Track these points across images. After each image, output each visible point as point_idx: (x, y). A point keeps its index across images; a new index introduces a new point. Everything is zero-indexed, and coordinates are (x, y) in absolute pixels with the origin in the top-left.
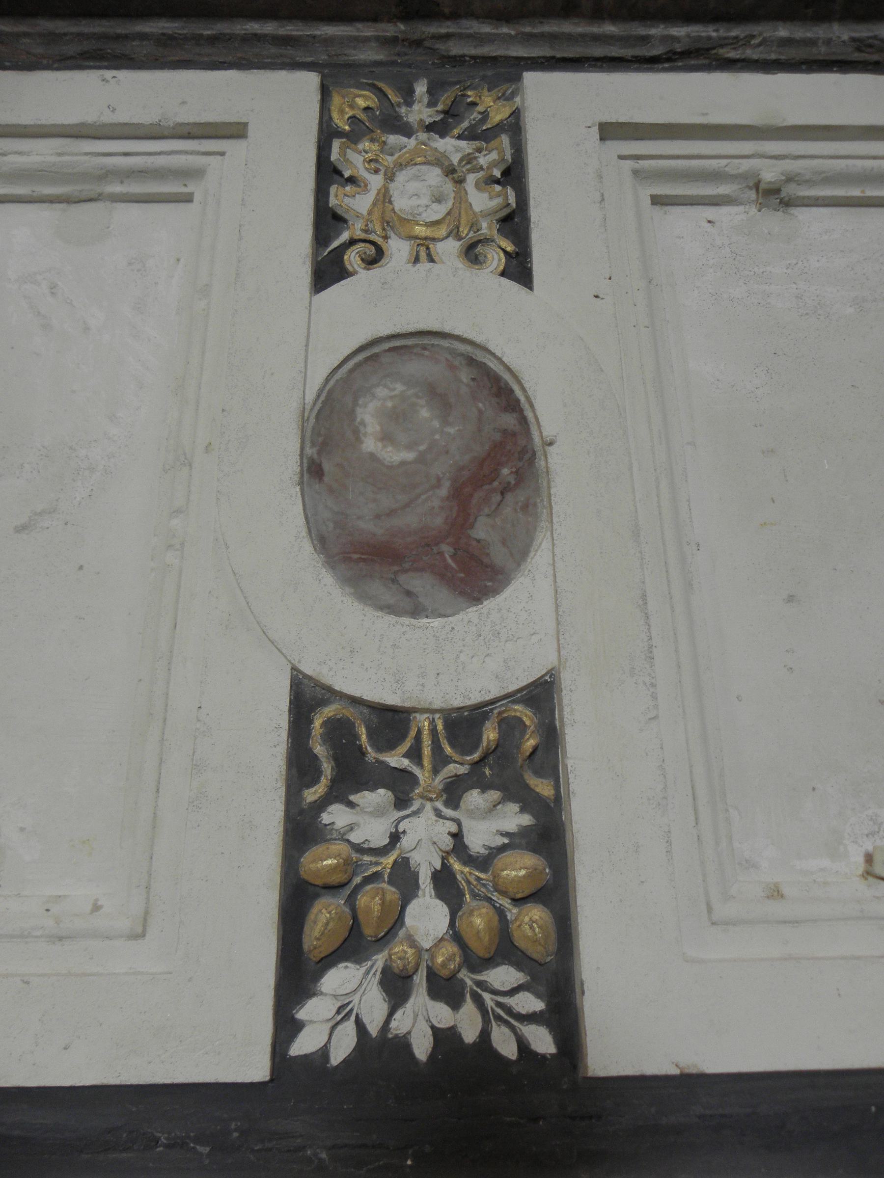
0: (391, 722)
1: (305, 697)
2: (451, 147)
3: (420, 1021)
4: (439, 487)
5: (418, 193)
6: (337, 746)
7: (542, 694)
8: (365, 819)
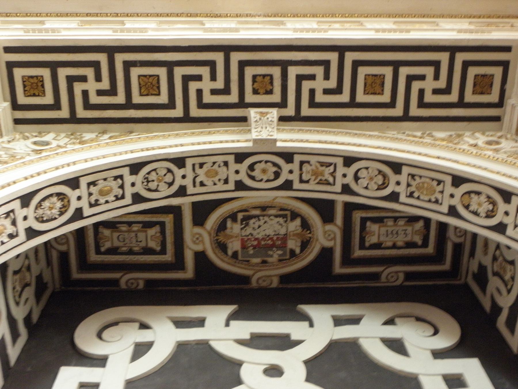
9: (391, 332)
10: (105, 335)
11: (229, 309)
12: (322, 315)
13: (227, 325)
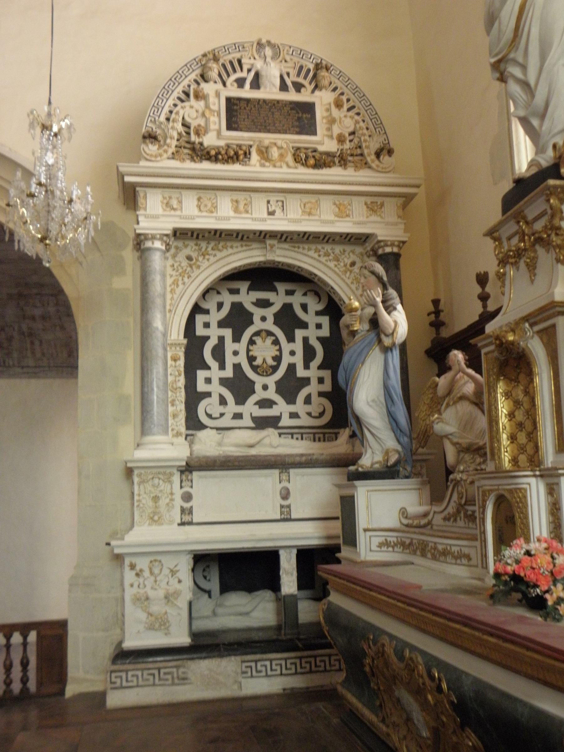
4: (286, 494)
5: (284, 478)
6: (282, 507)
8: (283, 509)
9: (304, 300)
10: (206, 297)
12: (281, 287)
13: (248, 293)
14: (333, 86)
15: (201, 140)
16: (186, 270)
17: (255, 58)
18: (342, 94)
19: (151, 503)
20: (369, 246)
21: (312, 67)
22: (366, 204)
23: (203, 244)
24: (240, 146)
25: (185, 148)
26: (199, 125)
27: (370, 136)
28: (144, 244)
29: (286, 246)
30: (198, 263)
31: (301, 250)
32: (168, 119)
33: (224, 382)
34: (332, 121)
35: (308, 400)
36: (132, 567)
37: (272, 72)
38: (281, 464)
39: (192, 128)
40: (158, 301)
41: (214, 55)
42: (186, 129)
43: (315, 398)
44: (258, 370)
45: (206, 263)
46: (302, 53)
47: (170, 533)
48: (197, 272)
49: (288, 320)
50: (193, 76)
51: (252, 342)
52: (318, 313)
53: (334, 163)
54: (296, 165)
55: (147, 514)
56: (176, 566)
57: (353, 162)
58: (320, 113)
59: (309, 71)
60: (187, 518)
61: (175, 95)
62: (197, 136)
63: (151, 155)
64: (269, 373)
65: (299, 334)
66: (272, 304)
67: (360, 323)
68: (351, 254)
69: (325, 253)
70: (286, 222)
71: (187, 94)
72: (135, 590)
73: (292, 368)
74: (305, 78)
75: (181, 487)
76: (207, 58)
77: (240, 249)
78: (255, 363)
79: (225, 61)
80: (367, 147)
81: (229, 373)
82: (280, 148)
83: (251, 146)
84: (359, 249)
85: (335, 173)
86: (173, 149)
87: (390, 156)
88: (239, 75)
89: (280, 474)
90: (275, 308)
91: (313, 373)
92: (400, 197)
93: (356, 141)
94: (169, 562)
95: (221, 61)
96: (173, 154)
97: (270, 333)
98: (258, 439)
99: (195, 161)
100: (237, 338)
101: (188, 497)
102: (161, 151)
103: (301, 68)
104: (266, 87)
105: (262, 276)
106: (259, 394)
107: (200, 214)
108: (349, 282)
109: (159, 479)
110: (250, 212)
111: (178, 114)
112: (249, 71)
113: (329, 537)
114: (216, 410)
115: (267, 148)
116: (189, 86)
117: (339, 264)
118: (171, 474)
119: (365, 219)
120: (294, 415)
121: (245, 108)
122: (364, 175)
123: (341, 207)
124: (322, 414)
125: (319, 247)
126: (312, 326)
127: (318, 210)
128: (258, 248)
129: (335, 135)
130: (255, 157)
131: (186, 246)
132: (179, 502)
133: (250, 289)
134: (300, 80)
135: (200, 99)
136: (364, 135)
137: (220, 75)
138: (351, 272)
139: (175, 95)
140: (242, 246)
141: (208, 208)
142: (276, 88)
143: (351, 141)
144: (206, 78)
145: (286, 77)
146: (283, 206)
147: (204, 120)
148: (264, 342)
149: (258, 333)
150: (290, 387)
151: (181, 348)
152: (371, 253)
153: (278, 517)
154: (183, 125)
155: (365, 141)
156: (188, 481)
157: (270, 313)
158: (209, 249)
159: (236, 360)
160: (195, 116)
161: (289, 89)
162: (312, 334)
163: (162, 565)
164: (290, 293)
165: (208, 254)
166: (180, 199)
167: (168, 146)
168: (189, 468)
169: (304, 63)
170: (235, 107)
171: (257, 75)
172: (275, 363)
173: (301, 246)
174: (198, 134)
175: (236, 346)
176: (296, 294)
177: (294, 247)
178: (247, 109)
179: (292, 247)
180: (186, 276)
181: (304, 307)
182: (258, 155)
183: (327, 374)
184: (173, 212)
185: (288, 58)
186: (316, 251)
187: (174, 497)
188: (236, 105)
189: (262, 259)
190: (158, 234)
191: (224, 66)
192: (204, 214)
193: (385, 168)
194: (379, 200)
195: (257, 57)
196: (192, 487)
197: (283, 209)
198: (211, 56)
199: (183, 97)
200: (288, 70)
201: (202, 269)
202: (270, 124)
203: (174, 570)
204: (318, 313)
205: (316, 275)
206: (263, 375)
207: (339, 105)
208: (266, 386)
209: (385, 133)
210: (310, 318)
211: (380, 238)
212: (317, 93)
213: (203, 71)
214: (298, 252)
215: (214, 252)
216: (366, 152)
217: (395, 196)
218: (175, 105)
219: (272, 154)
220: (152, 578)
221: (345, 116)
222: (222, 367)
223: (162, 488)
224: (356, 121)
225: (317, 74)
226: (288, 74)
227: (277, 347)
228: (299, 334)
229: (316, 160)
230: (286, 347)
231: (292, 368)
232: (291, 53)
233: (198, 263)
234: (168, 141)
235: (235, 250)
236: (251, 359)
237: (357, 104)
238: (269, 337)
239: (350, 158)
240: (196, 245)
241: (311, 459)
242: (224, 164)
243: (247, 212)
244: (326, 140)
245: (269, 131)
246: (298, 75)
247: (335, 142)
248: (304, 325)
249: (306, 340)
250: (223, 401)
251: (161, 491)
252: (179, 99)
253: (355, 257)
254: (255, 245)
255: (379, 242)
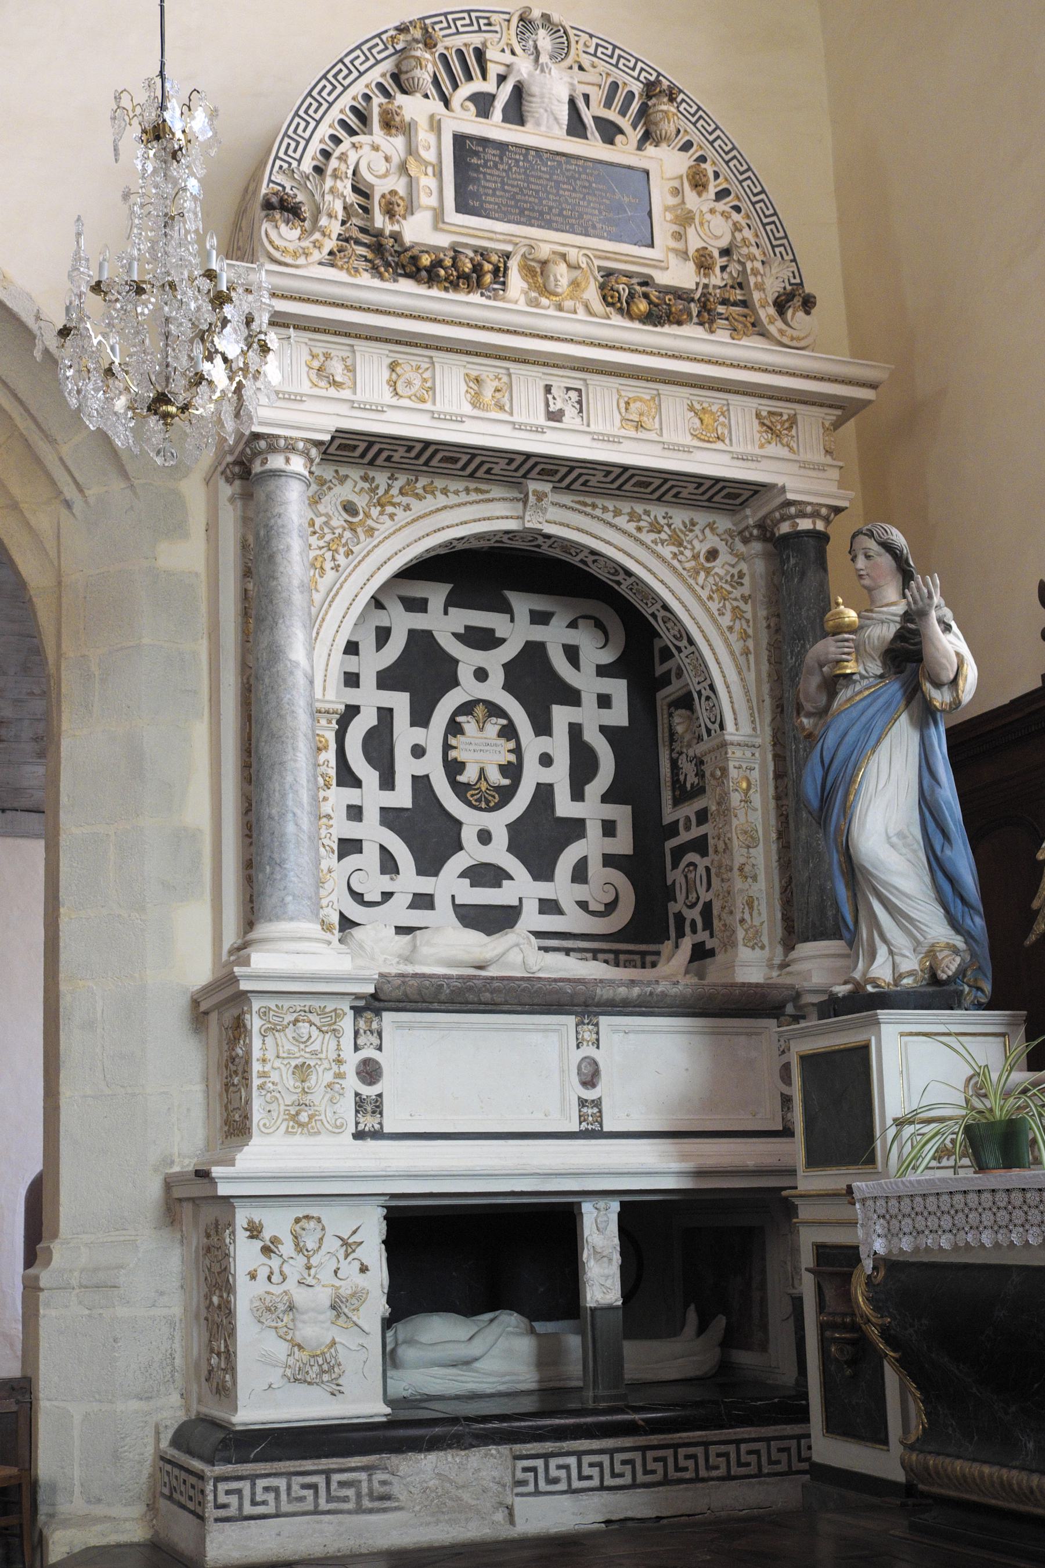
0: (586, 1101)
1: (579, 1098)
2: (590, 1027)
3: (590, 1127)
4: (590, 1077)
5: (587, 1035)
6: (583, 1103)
7: (600, 1098)
8: (585, 1110)
9: (573, 637)
11: (448, 587)
12: (522, 603)
13: (446, 613)
14: (683, 139)
15: (396, 228)
16: (341, 536)
17: (513, 53)
18: (702, 159)
19: (291, 1082)
20: (751, 516)
21: (637, 88)
22: (758, 416)
23: (381, 478)
24: (483, 253)
25: (357, 242)
26: (393, 193)
27: (763, 263)
28: (264, 462)
29: (567, 499)
30: (370, 522)
31: (598, 512)
32: (319, 170)
33: (390, 817)
34: (685, 219)
35: (580, 874)
36: (254, 1231)
37: (554, 88)
38: (580, 1004)
39: (377, 198)
40: (298, 599)
41: (425, 29)
42: (362, 201)
43: (595, 867)
44: (468, 795)
45: (386, 526)
46: (614, 54)
47: (332, 1153)
48: (366, 543)
49: (537, 683)
50: (375, 75)
51: (454, 728)
52: (602, 671)
53: (690, 314)
54: (608, 309)
55: (282, 1108)
56: (354, 1232)
57: (727, 319)
58: (660, 198)
59: (631, 95)
60: (369, 1122)
61: (334, 114)
62: (387, 218)
63: (285, 251)
64: (492, 804)
65: (561, 716)
66: (503, 641)
67: (857, 661)
68: (707, 531)
69: (651, 524)
70: (586, 440)
71: (363, 117)
72: (260, 1286)
73: (544, 793)
74: (623, 113)
75: (357, 1048)
76: (409, 38)
77: (463, 497)
78: (461, 778)
79: (447, 48)
80: (760, 287)
81: (402, 797)
82: (573, 267)
83: (507, 256)
84: (724, 523)
85: (689, 336)
86: (330, 244)
87: (808, 313)
88: (478, 85)
89: (577, 1025)
90: (508, 652)
91: (591, 809)
92: (831, 406)
93: (734, 268)
94: (338, 1221)
95: (440, 49)
96: (331, 253)
97: (495, 710)
98: (499, 950)
99: (381, 277)
100: (421, 717)
101: (370, 1072)
102: (306, 244)
103: (615, 86)
104: (538, 124)
105: (472, 572)
106: (472, 853)
107: (394, 401)
108: (704, 594)
109: (311, 1024)
110: (507, 408)
111: (346, 161)
112: (502, 79)
113: (700, 1173)
114: (373, 885)
115: (544, 263)
116: (367, 98)
117: (682, 553)
118: (338, 1014)
119: (758, 451)
120: (549, 907)
121: (496, 166)
122: (752, 349)
123: (706, 418)
124: (611, 907)
125: (639, 508)
126: (589, 700)
127: (657, 419)
128: (504, 499)
129: (691, 252)
130: (516, 280)
131: (343, 479)
132: (353, 1083)
133: (451, 602)
134: (612, 115)
135: (394, 131)
136: (753, 259)
137: (436, 82)
138: (708, 571)
139: (334, 114)
140: (467, 490)
141: (414, 390)
142: (561, 128)
143: (723, 269)
144: (406, 85)
145: (581, 104)
146: (580, 402)
147: (404, 180)
148: (481, 729)
149: (466, 708)
150: (541, 839)
151: (329, 722)
152: (755, 532)
153: (574, 1127)
154: (356, 189)
155: (755, 272)
156: (372, 1032)
157: (495, 660)
158: (395, 491)
159: (420, 768)
160: (383, 171)
161: (589, 135)
162: (590, 718)
163: (323, 1229)
164: (540, 618)
165: (394, 505)
166: (349, 362)
167: (324, 234)
168: (374, 1004)
169: (620, 77)
170: (474, 160)
171: (519, 91)
172: (506, 782)
173: (599, 502)
174: (390, 212)
175: (418, 735)
176: (554, 621)
177: (585, 504)
178: (501, 167)
179: (579, 502)
180: (342, 550)
181: (572, 654)
182: (524, 278)
183: (622, 814)
184: (332, 392)
185: (586, 61)
186: (633, 517)
187: (343, 1068)
188: (476, 154)
189: (512, 525)
190: (302, 439)
191: (443, 57)
192: (405, 402)
193: (799, 339)
194: (786, 409)
195: (518, 50)
196: (380, 1048)
197: (581, 411)
198: (417, 34)
199: (353, 121)
200: (588, 89)
201: (378, 536)
202: (551, 208)
203: (350, 1241)
204: (602, 671)
205: (629, 573)
206: (481, 809)
207: (698, 184)
208: (486, 833)
209: (794, 260)
210: (584, 681)
211: (790, 496)
212: (650, 150)
213: (397, 66)
214: (593, 517)
215: (405, 500)
216: (756, 296)
217: (822, 405)
218: (336, 140)
219: (556, 280)
220: (301, 1260)
221: (712, 211)
222: (388, 782)
223: (316, 1046)
224: (734, 224)
225: (650, 105)
226: (587, 97)
227: (512, 745)
228: (561, 716)
229: (650, 303)
230: (533, 745)
231: (544, 793)
232: (592, 50)
233: (370, 522)
234: (323, 221)
235: (453, 499)
236: (453, 768)
237: (735, 188)
238: (494, 720)
239: (721, 309)
240: (365, 478)
241: (651, 994)
242: (446, 289)
243: (501, 408)
244: (673, 260)
245: (548, 225)
246: (608, 104)
247: (691, 266)
248: (572, 697)
249: (575, 731)
250: (389, 864)
251: (314, 1053)
252: (343, 123)
253: (717, 539)
254: (497, 492)
255: (789, 503)
